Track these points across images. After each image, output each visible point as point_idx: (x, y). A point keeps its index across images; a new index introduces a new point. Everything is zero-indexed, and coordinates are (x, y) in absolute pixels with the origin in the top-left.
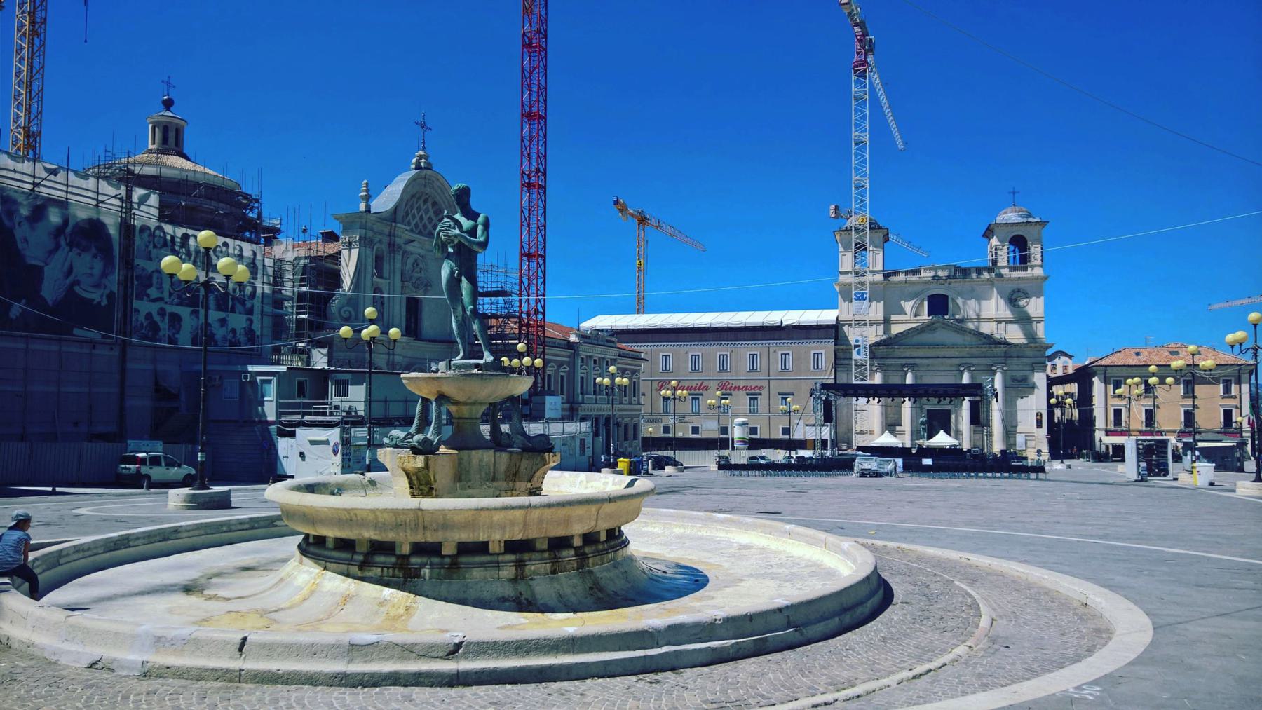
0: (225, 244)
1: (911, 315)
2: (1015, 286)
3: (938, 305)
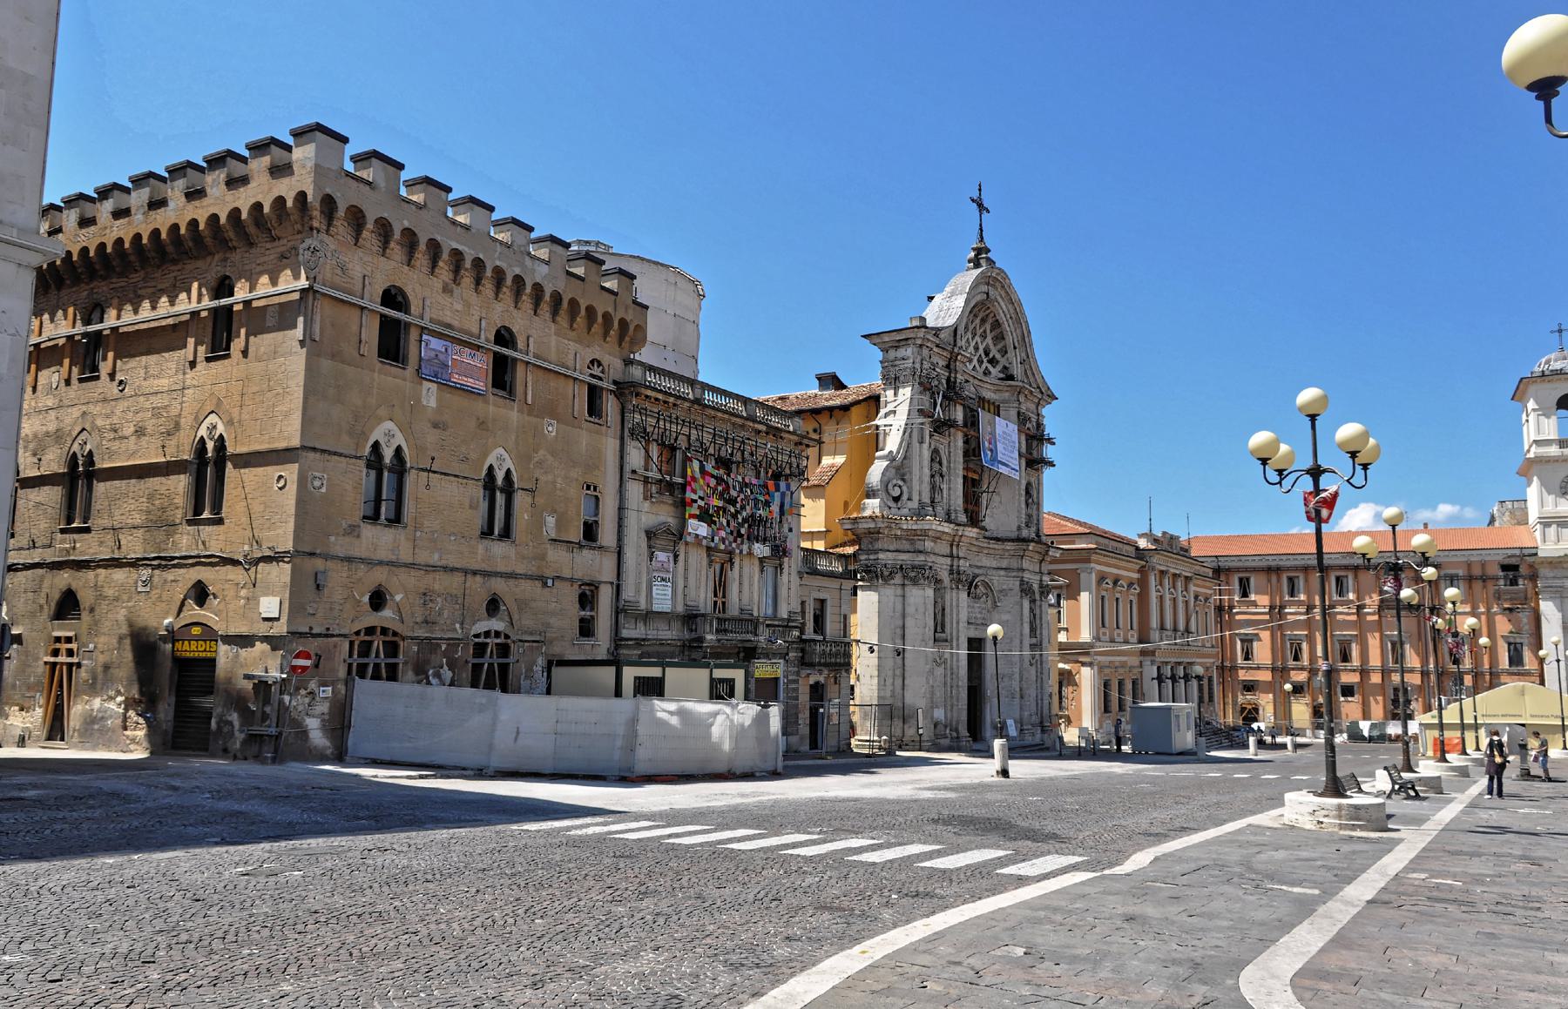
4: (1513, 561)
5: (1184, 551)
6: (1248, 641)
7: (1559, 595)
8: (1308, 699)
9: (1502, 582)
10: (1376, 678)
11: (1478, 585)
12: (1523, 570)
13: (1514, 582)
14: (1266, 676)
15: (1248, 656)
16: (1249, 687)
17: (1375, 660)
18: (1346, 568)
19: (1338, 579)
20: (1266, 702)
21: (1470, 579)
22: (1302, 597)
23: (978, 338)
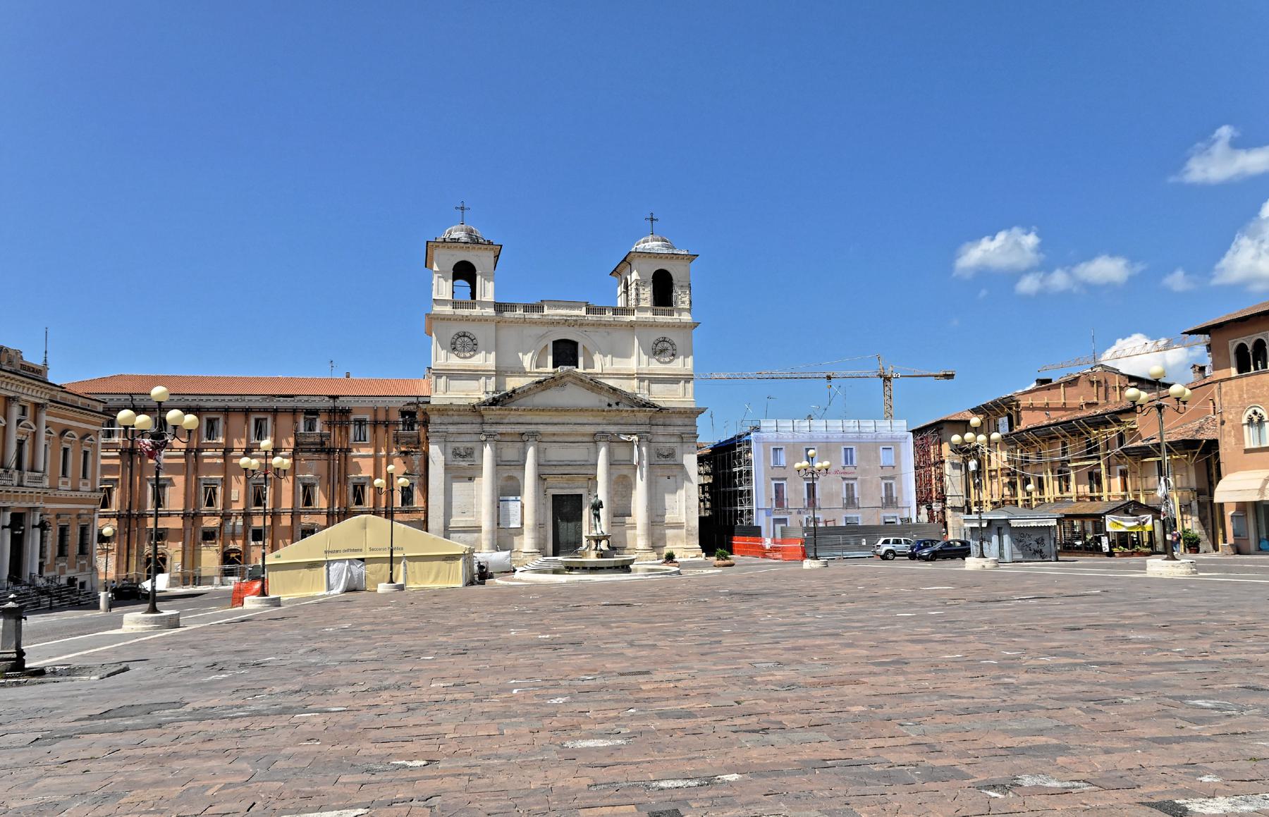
1: (534, 364)
2: (659, 334)
3: (566, 352)
4: (412, 408)
5: (35, 374)
6: (159, 488)
7: (445, 439)
8: (218, 546)
9: (401, 427)
10: (286, 521)
11: (381, 430)
12: (419, 417)
13: (411, 426)
14: (175, 523)
15: (159, 501)
16: (160, 535)
17: (287, 504)
18: (265, 410)
19: (257, 421)
20: (173, 551)
21: (375, 424)
22: (221, 440)
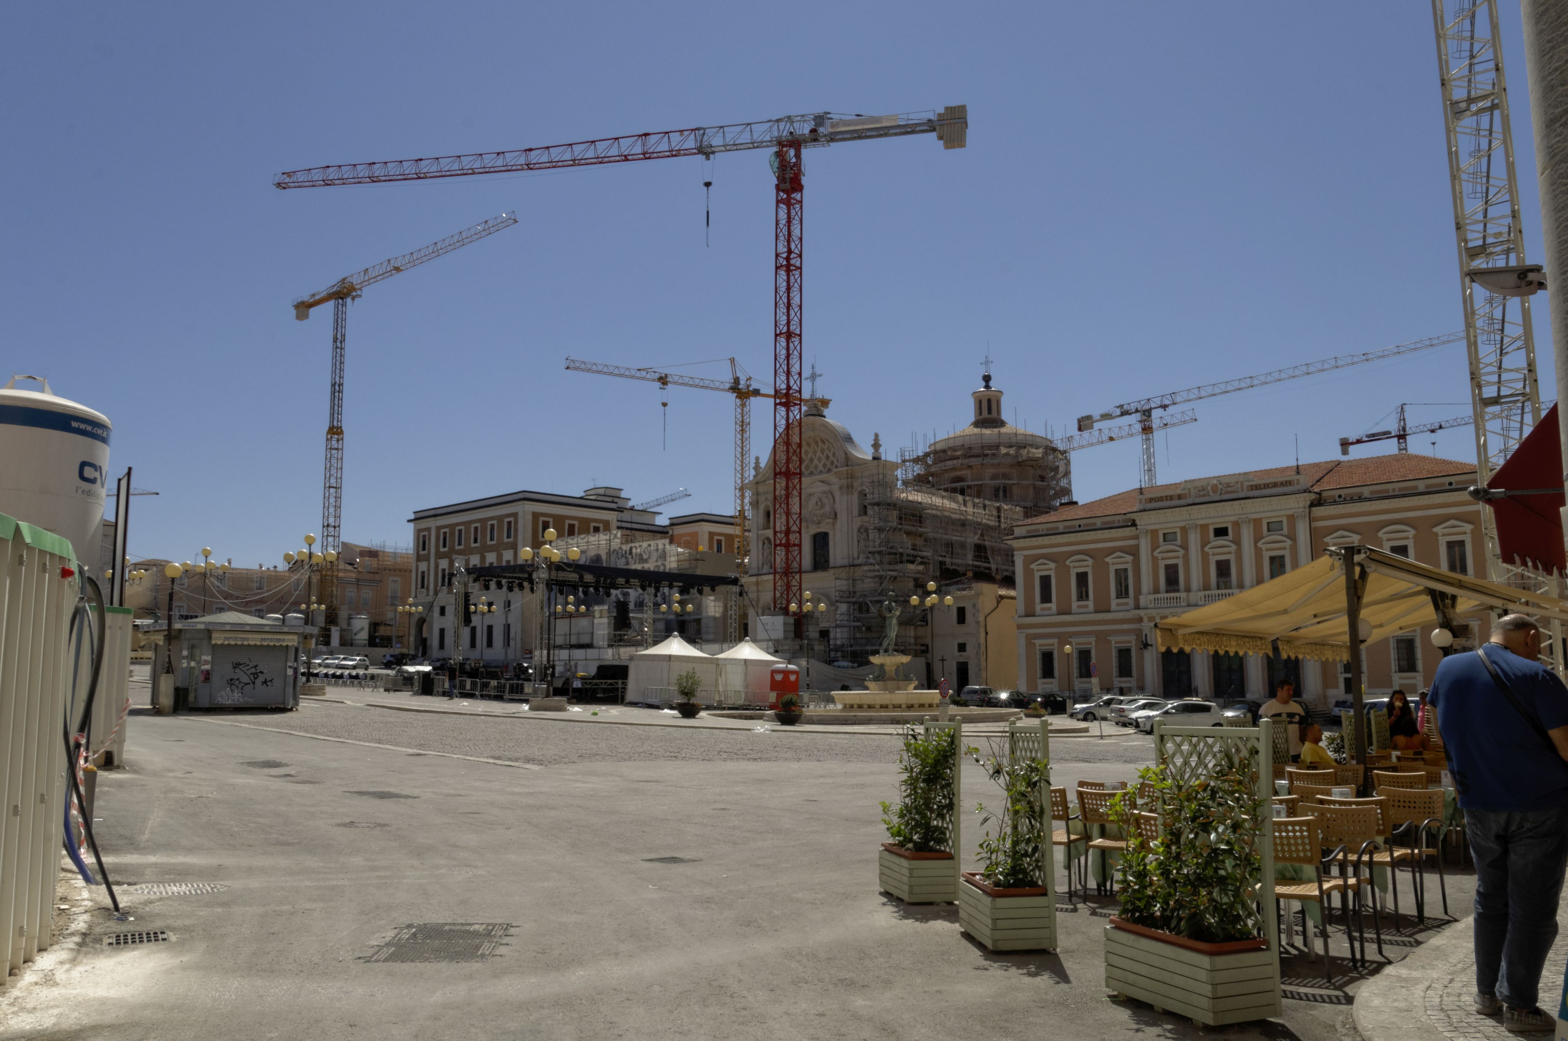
0: (649, 545)
23: (826, 452)
